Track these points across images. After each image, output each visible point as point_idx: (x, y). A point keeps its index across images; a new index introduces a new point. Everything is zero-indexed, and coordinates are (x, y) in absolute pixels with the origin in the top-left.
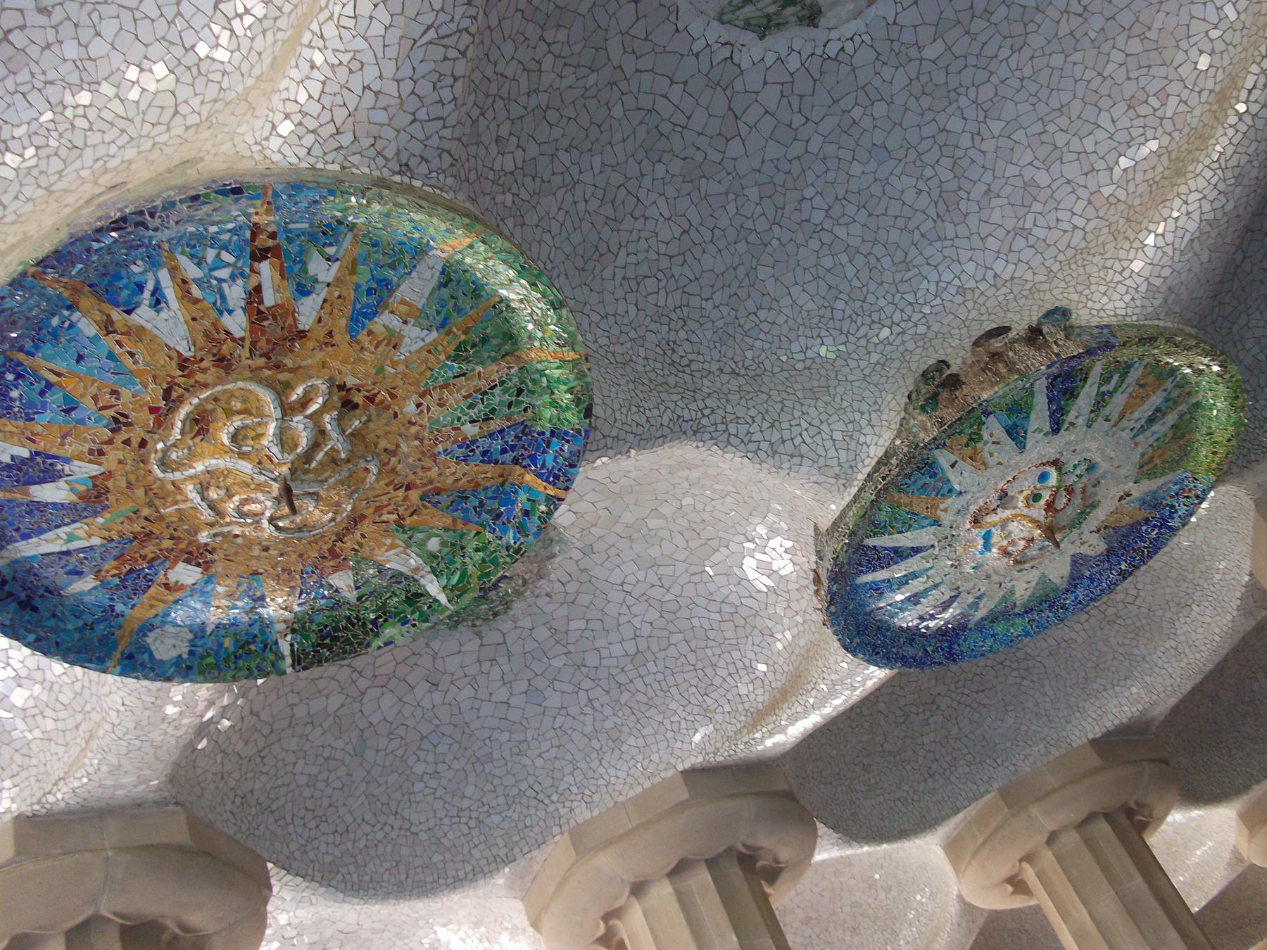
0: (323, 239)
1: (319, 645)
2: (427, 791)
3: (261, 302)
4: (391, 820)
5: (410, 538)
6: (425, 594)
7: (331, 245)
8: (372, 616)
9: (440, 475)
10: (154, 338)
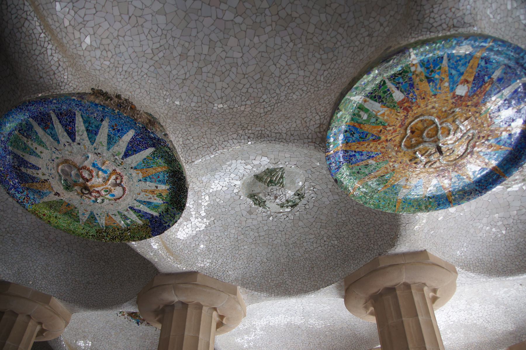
5: (377, 120)
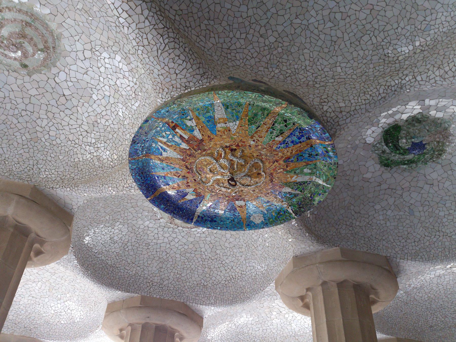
0: (184, 117)
1: (299, 208)
2: (449, 221)
3: (185, 138)
4: (438, 233)
5: (295, 172)
6: (320, 185)
7: (187, 116)
8: (309, 195)
9: (283, 154)
10: (172, 158)
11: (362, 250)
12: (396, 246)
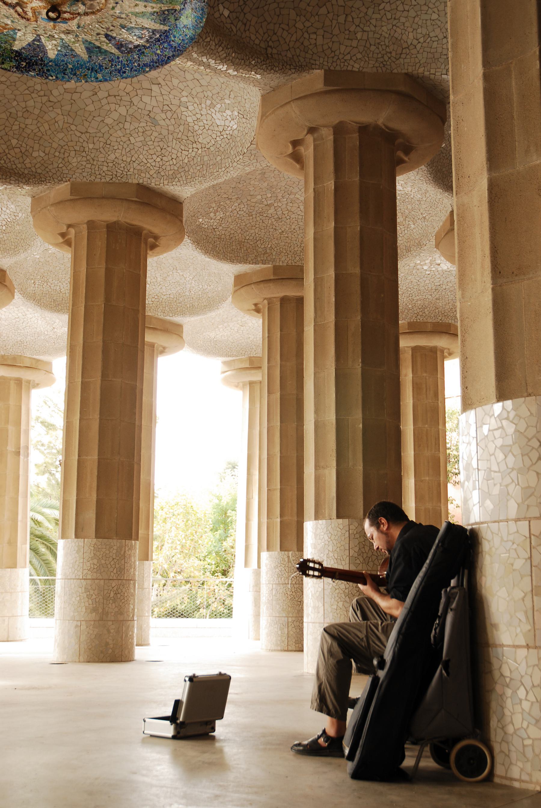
4: (195, 145)
11: (103, 180)
12: (151, 168)
